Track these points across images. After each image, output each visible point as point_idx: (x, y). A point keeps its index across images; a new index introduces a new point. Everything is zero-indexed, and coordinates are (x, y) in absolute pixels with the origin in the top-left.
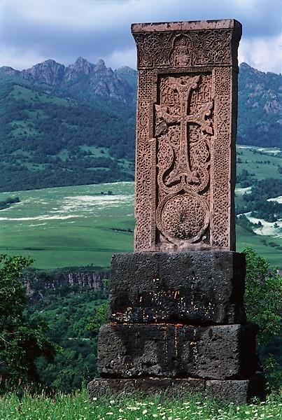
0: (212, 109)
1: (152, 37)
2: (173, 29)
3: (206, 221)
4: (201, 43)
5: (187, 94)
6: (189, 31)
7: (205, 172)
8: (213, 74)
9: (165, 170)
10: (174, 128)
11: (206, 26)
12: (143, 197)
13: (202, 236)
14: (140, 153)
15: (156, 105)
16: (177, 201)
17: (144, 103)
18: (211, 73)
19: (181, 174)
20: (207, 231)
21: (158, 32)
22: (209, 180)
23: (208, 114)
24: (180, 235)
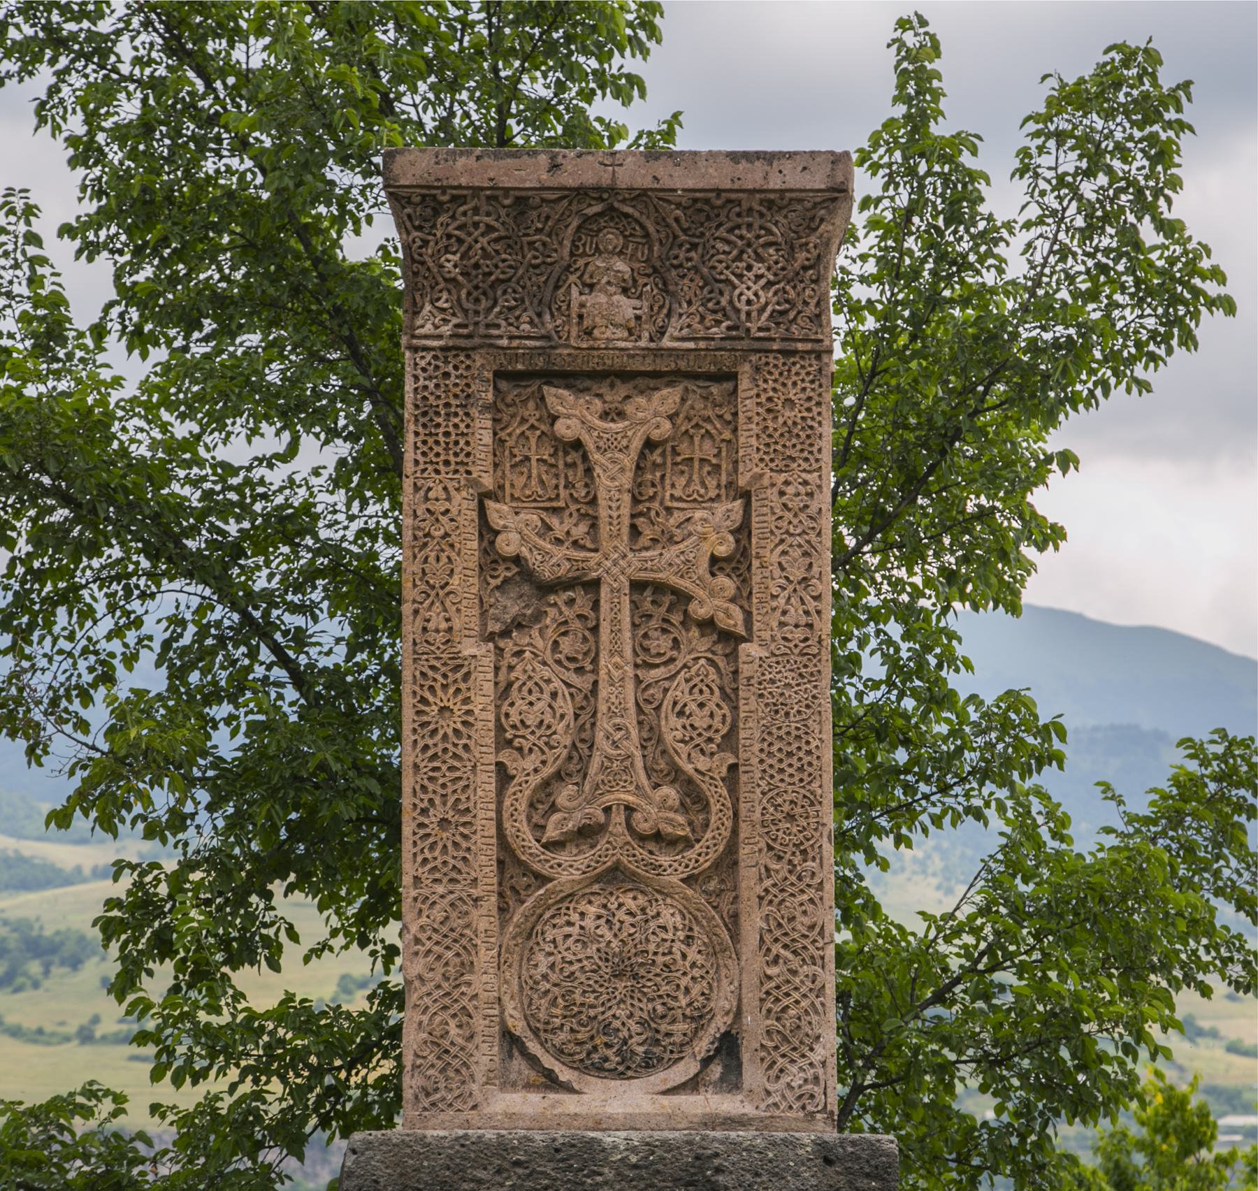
0: (743, 531)
1: (476, 210)
2: (571, 182)
3: (723, 1002)
4: (694, 247)
5: (628, 461)
6: (644, 192)
7: (717, 794)
8: (744, 383)
9: (535, 780)
10: (571, 602)
11: (717, 177)
12: (440, 889)
13: (706, 1062)
14: (424, 701)
15: (490, 504)
16: (592, 910)
17: (437, 492)
18: (733, 377)
19: (609, 799)
20: (728, 1046)
21: (507, 190)
22: (735, 832)
23: (722, 550)
24: (606, 1059)
